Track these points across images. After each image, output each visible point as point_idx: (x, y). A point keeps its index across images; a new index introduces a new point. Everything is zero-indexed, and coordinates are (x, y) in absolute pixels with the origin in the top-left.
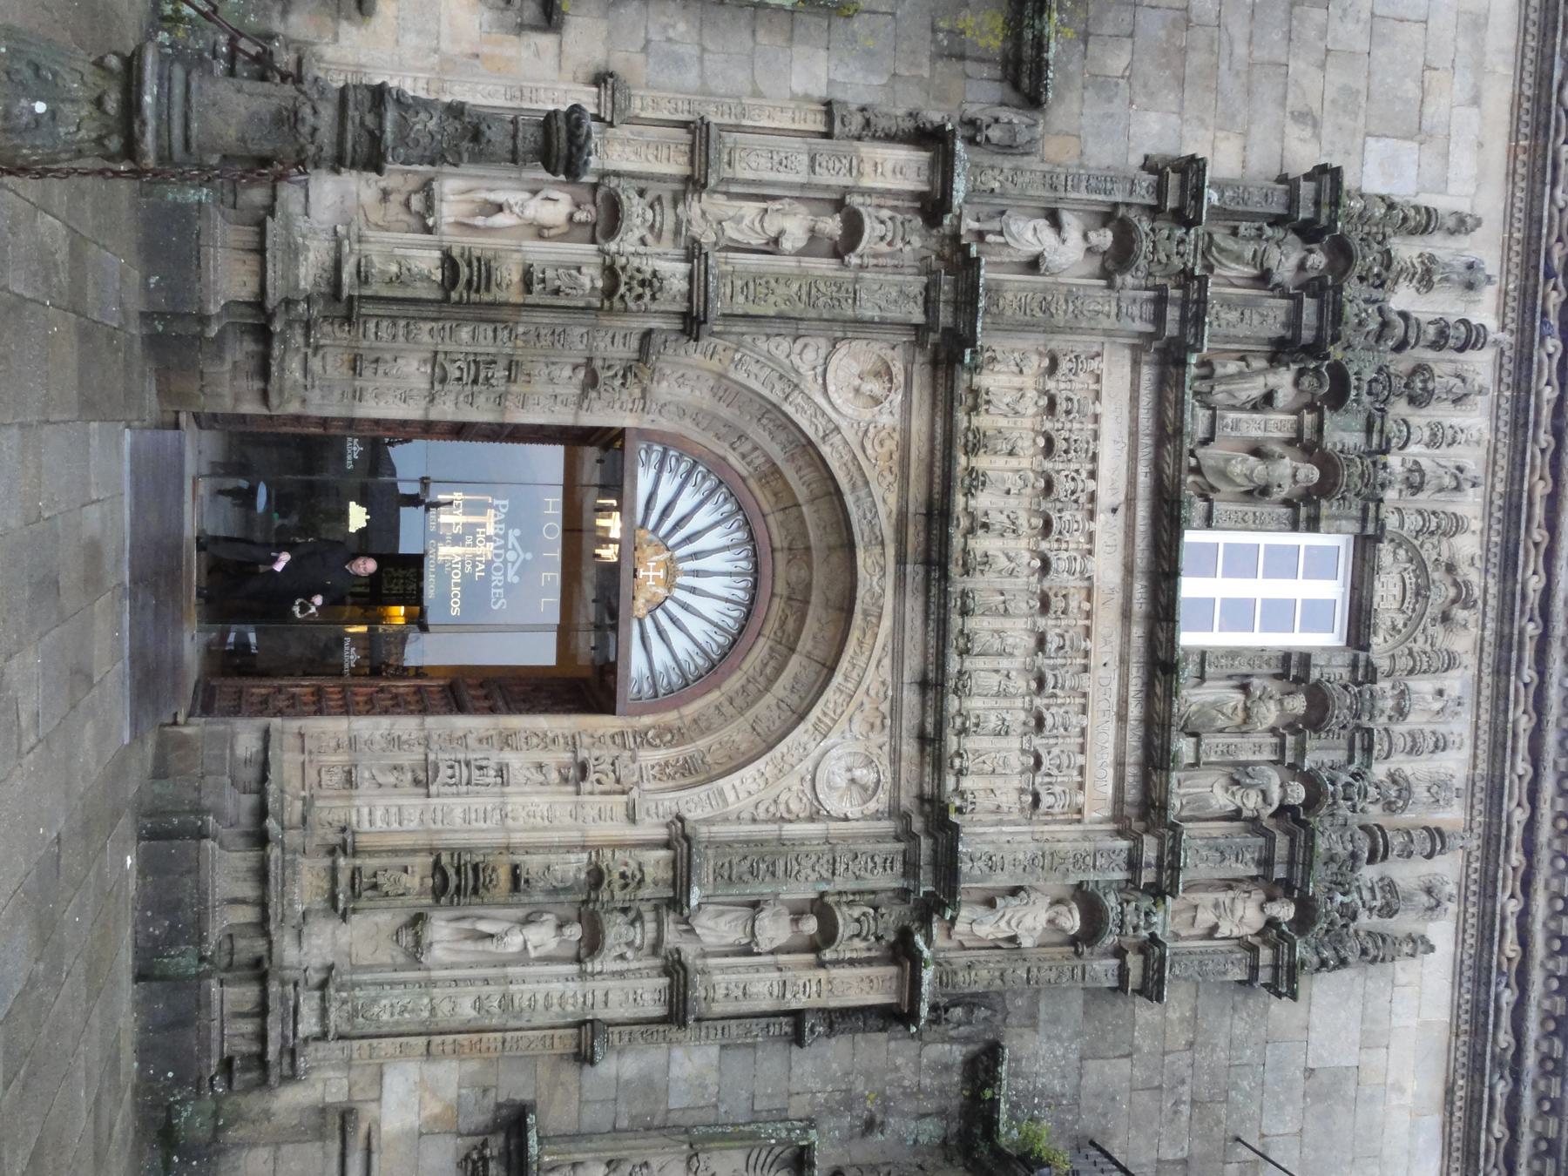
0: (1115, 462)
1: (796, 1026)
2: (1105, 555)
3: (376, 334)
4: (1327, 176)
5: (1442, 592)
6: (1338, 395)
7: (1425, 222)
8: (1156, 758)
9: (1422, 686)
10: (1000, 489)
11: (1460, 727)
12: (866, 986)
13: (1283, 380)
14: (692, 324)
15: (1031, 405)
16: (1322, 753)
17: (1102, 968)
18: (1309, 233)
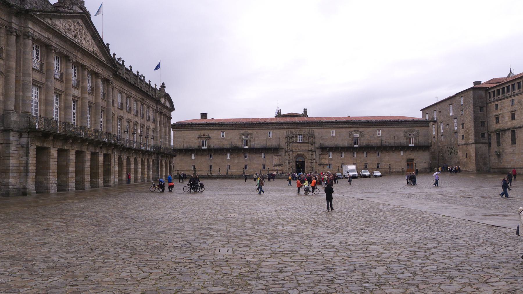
1: (316, 155)
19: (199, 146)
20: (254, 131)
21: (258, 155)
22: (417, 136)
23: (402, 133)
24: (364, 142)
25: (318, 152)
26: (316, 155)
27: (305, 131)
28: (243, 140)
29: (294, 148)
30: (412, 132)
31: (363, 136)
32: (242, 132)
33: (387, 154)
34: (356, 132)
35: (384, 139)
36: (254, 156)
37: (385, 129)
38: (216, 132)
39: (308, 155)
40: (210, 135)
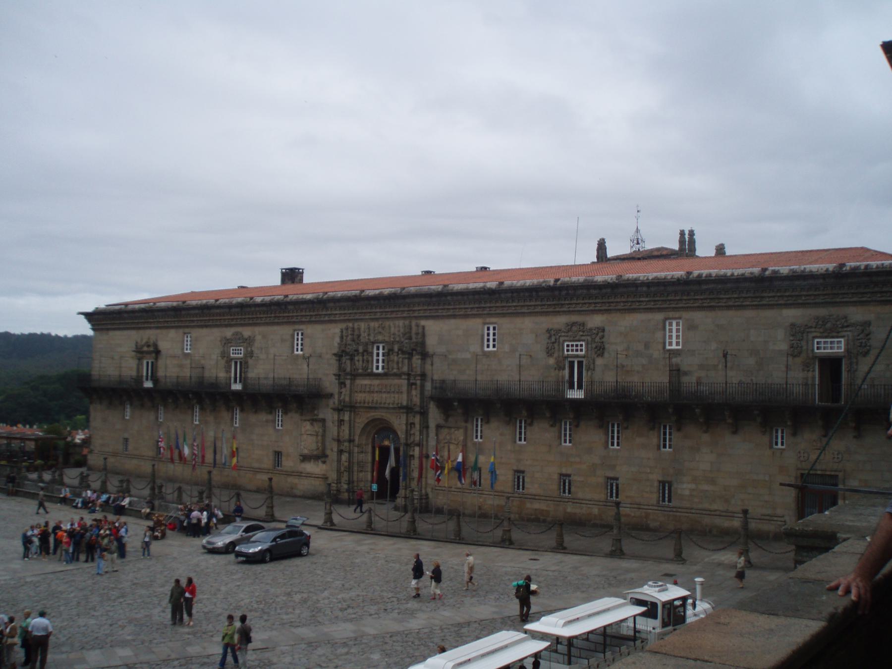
0: (366, 382)
2: (376, 382)
3: (355, 478)
4: (335, 355)
5: (380, 330)
6: (357, 351)
7: (342, 337)
8: (395, 375)
9: (392, 329)
10: (368, 397)
11: (397, 322)
12: (417, 419)
13: (356, 358)
14: (351, 441)
15: (360, 395)
16: (396, 348)
17: (418, 382)
18: (342, 356)
19: (139, 380)
20: (257, 330)
21: (263, 417)
22: (860, 348)
23: (780, 334)
24: (605, 376)
25: (435, 415)
26: (425, 426)
27: (396, 326)
28: (229, 360)
29: (359, 397)
30: (831, 330)
31: (600, 350)
32: (229, 332)
33: (706, 437)
34: (575, 331)
35: (685, 363)
36: (253, 418)
37: (698, 316)
38: (172, 333)
39: (399, 423)
40: (163, 345)
